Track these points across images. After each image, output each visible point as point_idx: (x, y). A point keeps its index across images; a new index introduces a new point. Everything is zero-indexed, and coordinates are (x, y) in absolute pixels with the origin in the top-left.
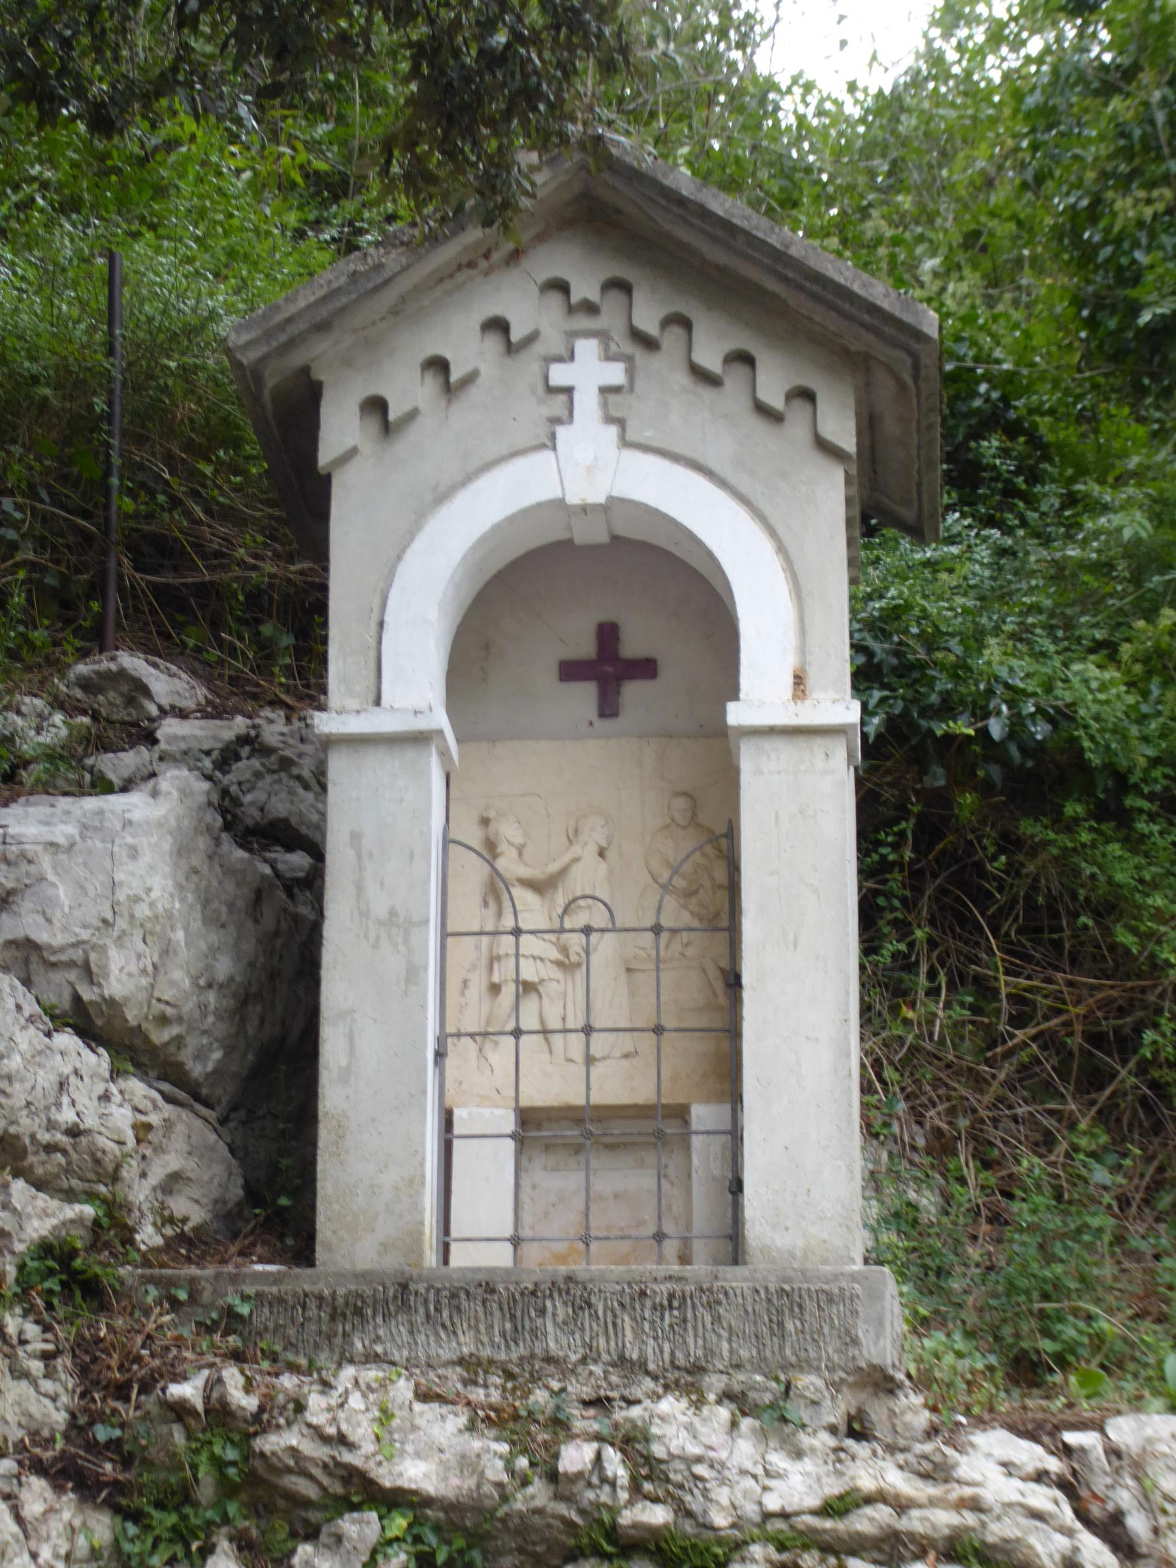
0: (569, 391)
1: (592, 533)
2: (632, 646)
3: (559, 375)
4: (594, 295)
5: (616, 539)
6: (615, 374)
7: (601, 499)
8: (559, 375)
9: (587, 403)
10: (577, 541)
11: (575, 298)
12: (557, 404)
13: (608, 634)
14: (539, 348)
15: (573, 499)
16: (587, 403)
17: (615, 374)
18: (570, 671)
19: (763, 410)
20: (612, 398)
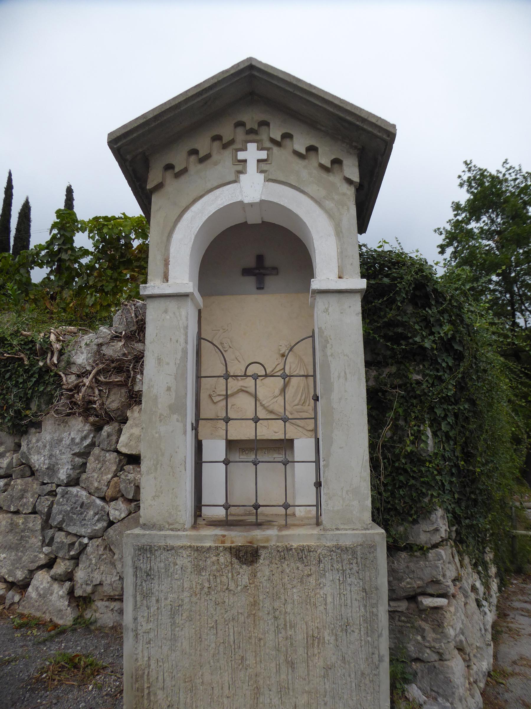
0: (245, 161)
1: (254, 219)
2: (269, 262)
3: (241, 155)
4: (256, 127)
5: (263, 222)
6: (263, 155)
7: (257, 200)
8: (241, 155)
9: (252, 166)
10: (249, 223)
11: (248, 127)
12: (239, 168)
13: (260, 258)
14: (235, 146)
15: (246, 201)
16: (252, 166)
17: (263, 155)
18: (246, 272)
19: (322, 167)
20: (261, 163)
